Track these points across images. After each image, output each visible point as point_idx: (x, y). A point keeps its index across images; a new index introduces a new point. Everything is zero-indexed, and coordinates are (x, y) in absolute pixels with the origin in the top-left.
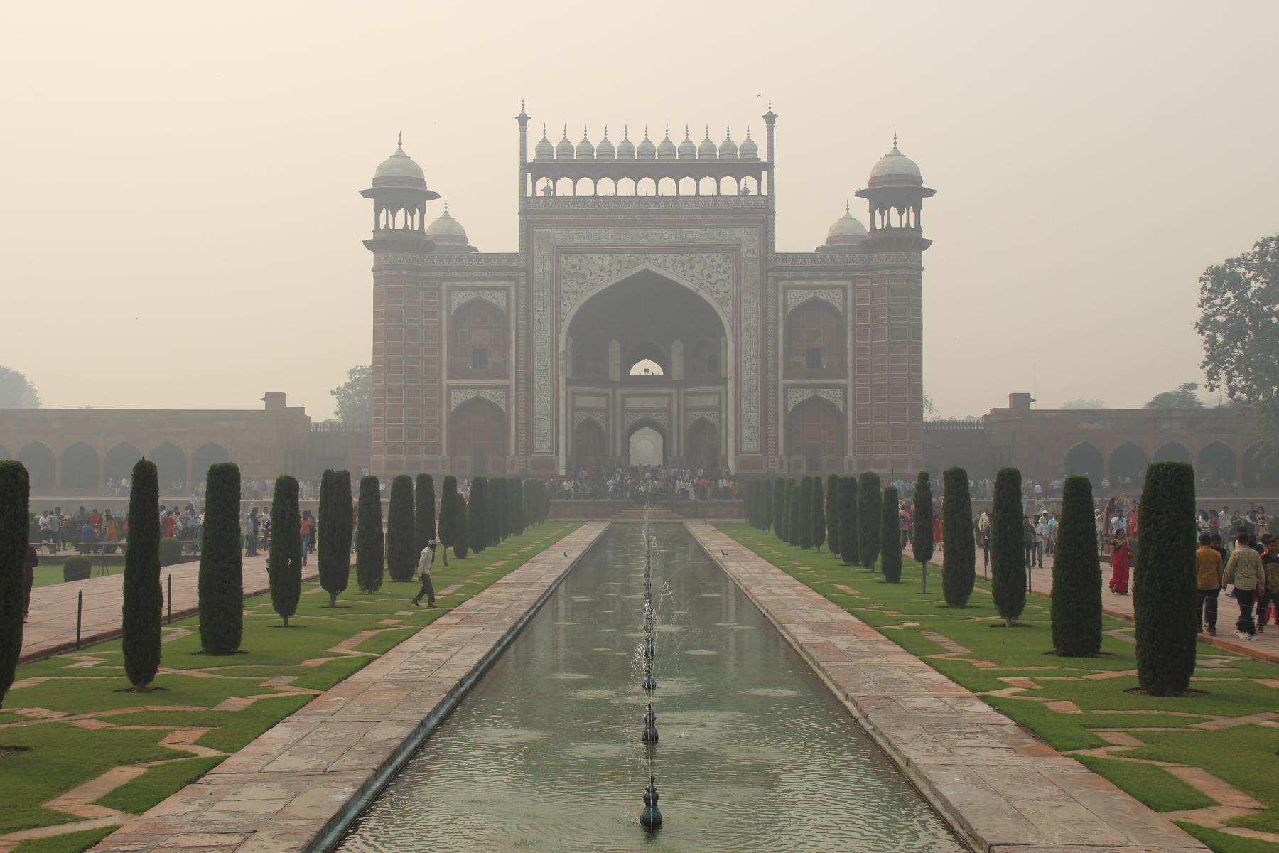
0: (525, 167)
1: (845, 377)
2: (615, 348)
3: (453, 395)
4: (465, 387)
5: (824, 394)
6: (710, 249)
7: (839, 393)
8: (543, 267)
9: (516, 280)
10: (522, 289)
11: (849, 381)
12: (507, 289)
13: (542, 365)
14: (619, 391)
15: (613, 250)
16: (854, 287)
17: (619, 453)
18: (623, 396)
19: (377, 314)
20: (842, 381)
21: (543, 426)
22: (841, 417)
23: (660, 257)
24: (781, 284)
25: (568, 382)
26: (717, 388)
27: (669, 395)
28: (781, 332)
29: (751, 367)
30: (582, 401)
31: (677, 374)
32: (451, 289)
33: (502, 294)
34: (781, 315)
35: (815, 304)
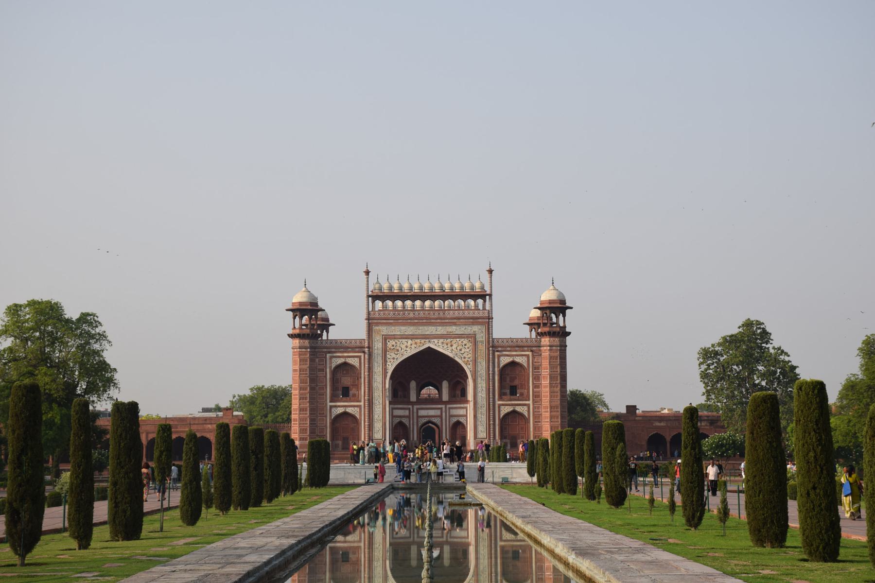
0: (369, 296)
1: (529, 400)
2: (413, 384)
3: (333, 410)
4: (339, 406)
5: (518, 409)
6: (460, 336)
7: (526, 408)
8: (378, 345)
9: (364, 352)
10: (366, 356)
11: (531, 402)
12: (359, 357)
13: (378, 395)
14: (415, 407)
15: (412, 337)
16: (533, 356)
17: (415, 439)
18: (418, 409)
19: (295, 371)
20: (527, 402)
21: (378, 426)
22: (527, 420)
23: (436, 341)
24: (497, 353)
25: (390, 403)
26: (465, 405)
27: (441, 409)
28: (497, 378)
29: (482, 395)
30: (397, 413)
31: (445, 397)
32: (331, 358)
33: (357, 360)
34: (496, 369)
35: (513, 364)
